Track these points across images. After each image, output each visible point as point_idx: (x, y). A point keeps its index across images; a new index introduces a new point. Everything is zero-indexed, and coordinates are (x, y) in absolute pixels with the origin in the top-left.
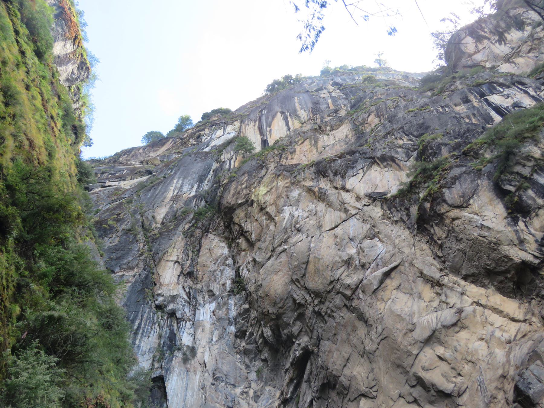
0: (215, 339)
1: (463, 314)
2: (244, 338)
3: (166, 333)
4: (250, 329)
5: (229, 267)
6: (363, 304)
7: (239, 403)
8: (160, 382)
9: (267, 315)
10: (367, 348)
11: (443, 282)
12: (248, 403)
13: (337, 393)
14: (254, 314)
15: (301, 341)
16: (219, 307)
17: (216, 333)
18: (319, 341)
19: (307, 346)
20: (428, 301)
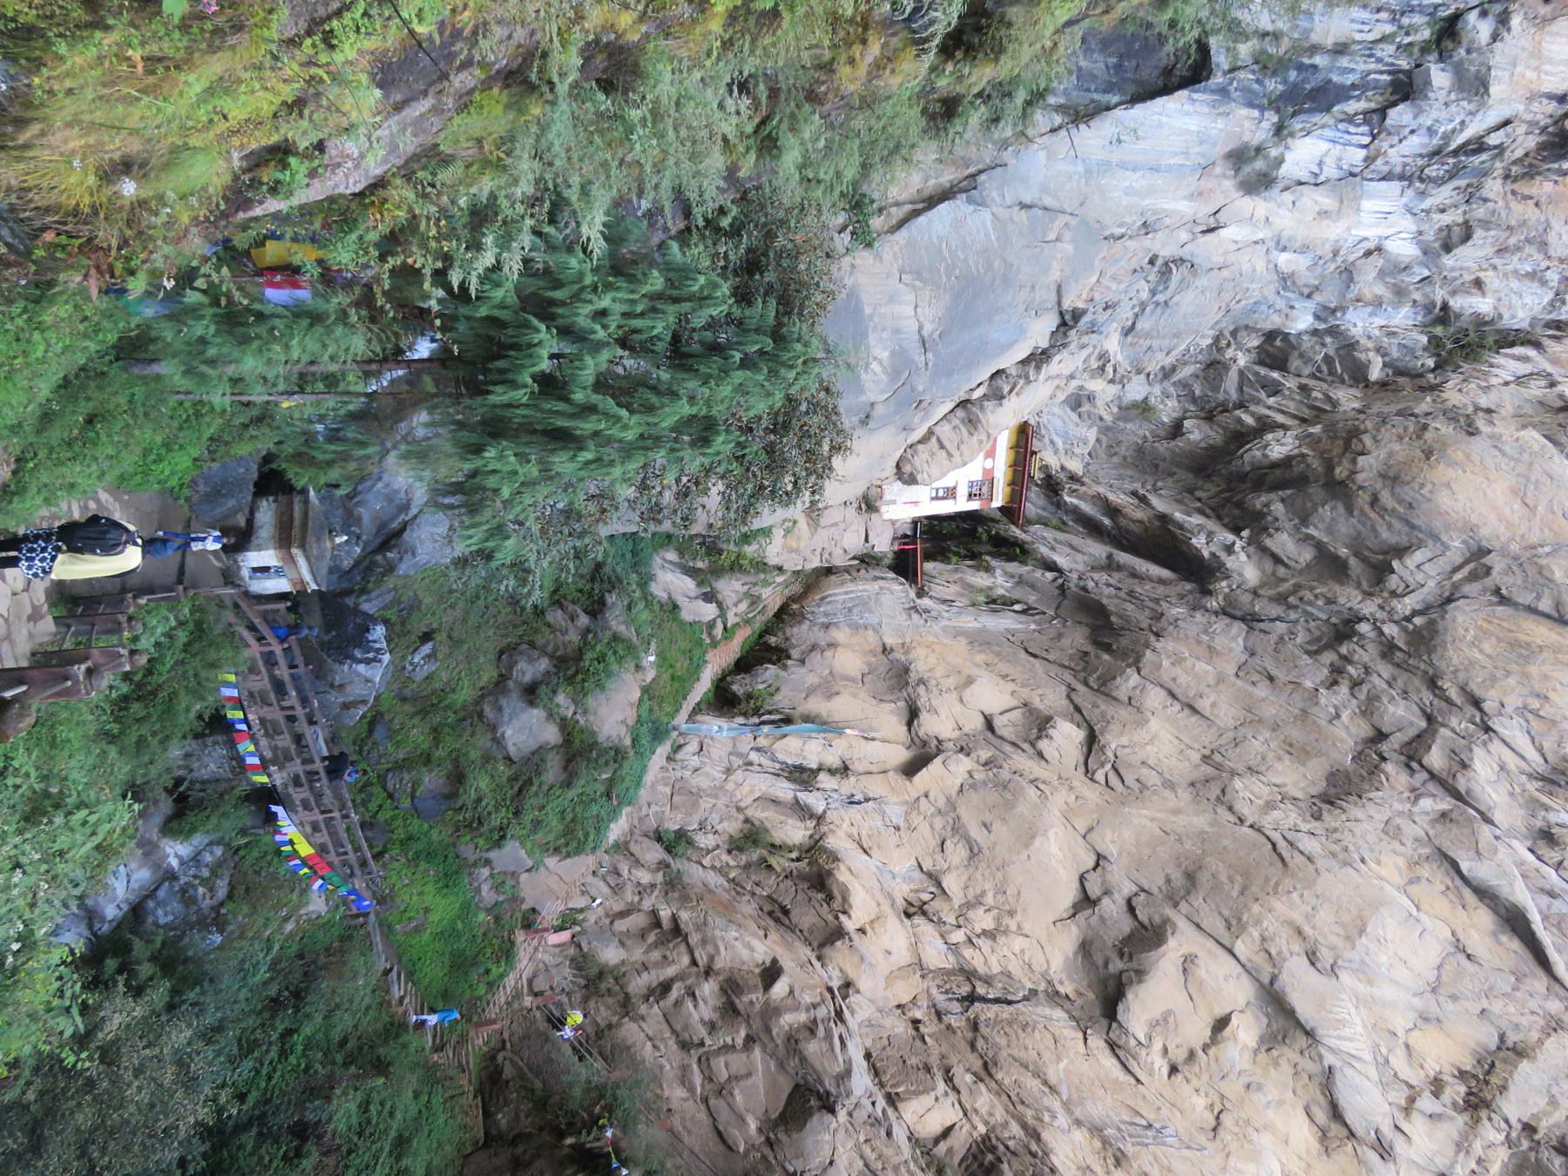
0: (1283, 259)
1: (1373, 1157)
2: (1261, 363)
4: (1291, 383)
5: (1552, 304)
6: (1397, 806)
7: (1083, 347)
8: (1192, 72)
9: (1347, 447)
10: (1238, 783)
11: (1485, 1121)
12: (1072, 377)
13: (1086, 654)
14: (1348, 399)
15: (1243, 556)
18: (1243, 619)
19: (1228, 577)
20: (1411, 1042)
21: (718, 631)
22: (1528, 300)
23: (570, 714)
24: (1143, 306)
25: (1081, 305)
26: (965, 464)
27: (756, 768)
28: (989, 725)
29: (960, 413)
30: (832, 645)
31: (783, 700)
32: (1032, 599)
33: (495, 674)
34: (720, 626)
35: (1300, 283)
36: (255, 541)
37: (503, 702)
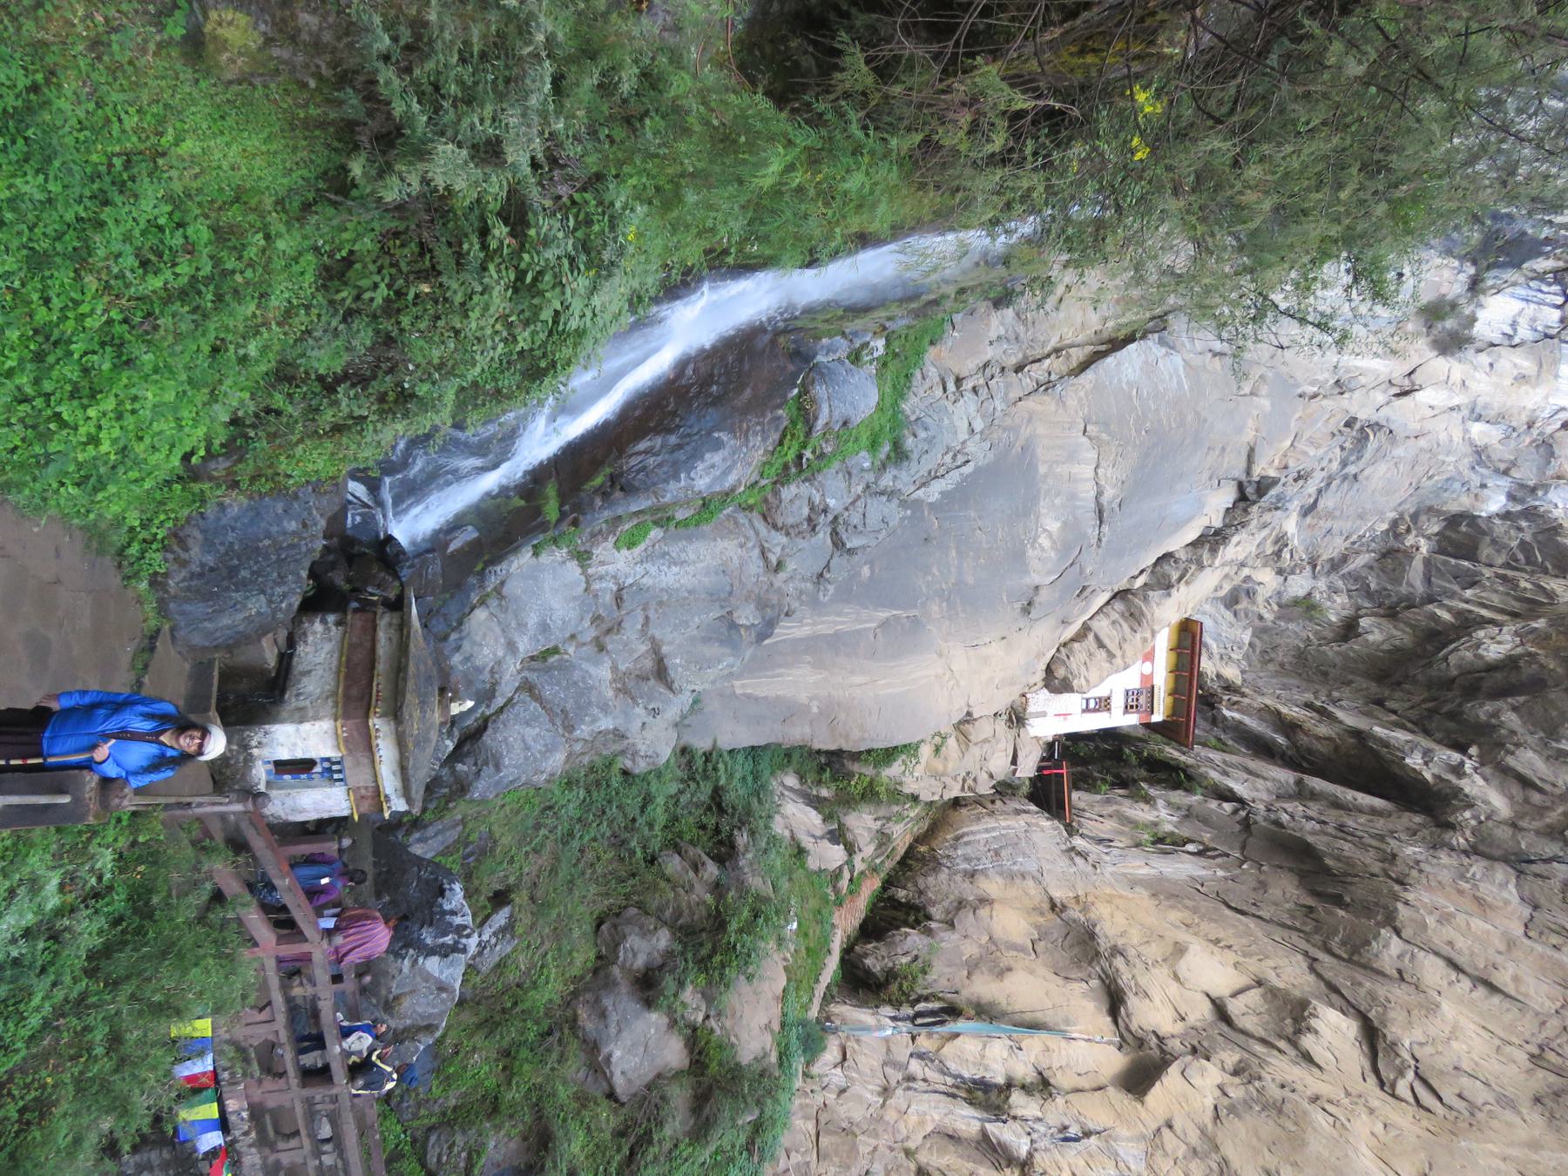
0: (1477, 429)
2: (1441, 551)
12: (1243, 565)
13: (1311, 909)
19: (1470, 806)
21: (844, 883)
23: (700, 1018)
24: (1329, 480)
25: (1272, 473)
26: (1126, 667)
27: (920, 1085)
28: (1221, 1011)
29: (1119, 606)
30: (984, 901)
31: (941, 978)
32: (1207, 836)
33: (592, 955)
34: (846, 875)
35: (1494, 457)
36: (291, 701)
37: (607, 1002)
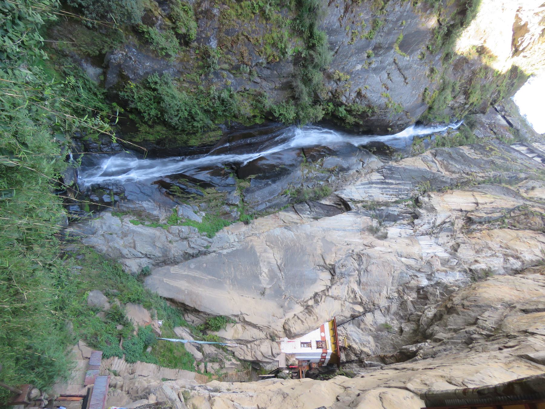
0: (403, 259)
3: (392, 211)
16: (445, 262)
17: (412, 262)
22: (496, 262)
25: (333, 263)
29: (306, 311)
